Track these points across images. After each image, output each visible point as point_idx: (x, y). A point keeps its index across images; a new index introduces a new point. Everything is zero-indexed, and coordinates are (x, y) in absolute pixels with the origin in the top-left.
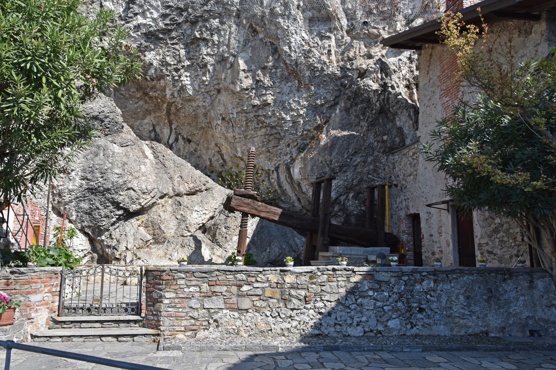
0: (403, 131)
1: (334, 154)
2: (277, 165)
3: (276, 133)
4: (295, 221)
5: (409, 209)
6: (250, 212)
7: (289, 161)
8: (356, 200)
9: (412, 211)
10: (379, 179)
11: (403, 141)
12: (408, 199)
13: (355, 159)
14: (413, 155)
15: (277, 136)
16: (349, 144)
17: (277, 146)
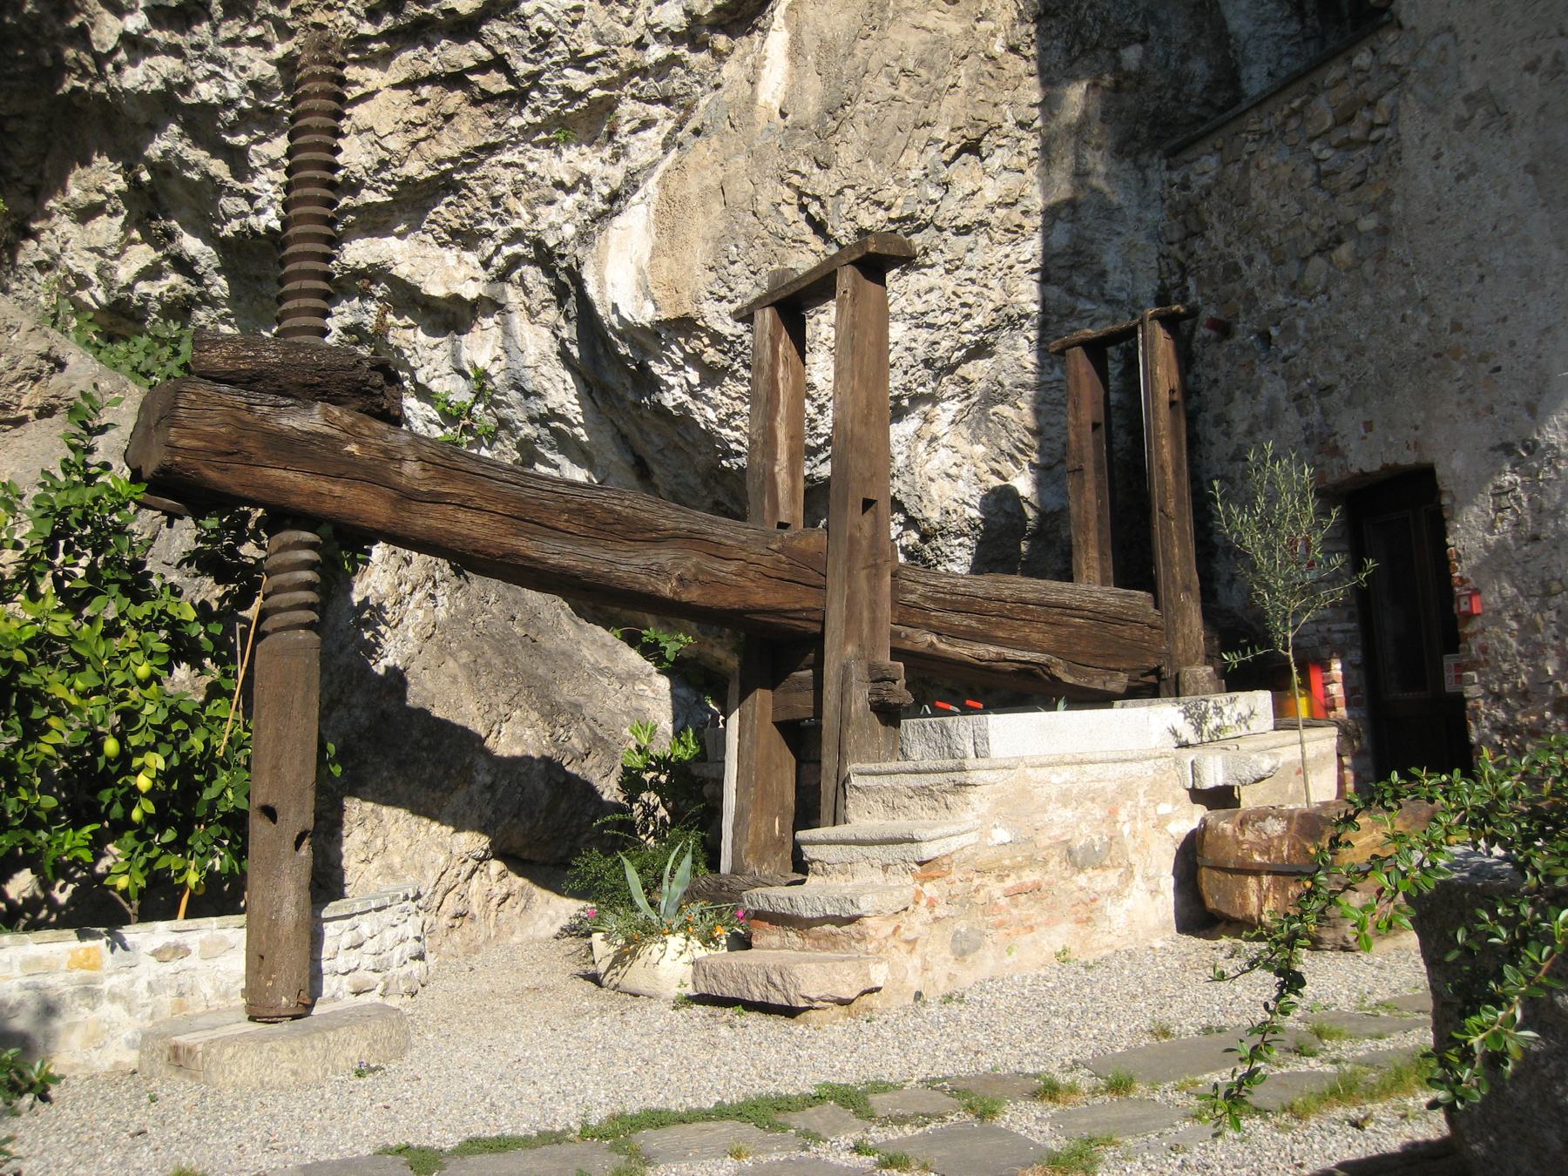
0: (1223, 23)
1: (846, 156)
2: (498, 261)
3: (482, 67)
4: (664, 556)
5: (1335, 451)
6: (329, 506)
7: (569, 231)
8: (975, 439)
9: (1364, 456)
10: (1104, 310)
11: (1228, 76)
12: (1328, 389)
13: (969, 186)
14: (1345, 119)
15: (495, 82)
16: (933, 95)
17: (491, 149)
